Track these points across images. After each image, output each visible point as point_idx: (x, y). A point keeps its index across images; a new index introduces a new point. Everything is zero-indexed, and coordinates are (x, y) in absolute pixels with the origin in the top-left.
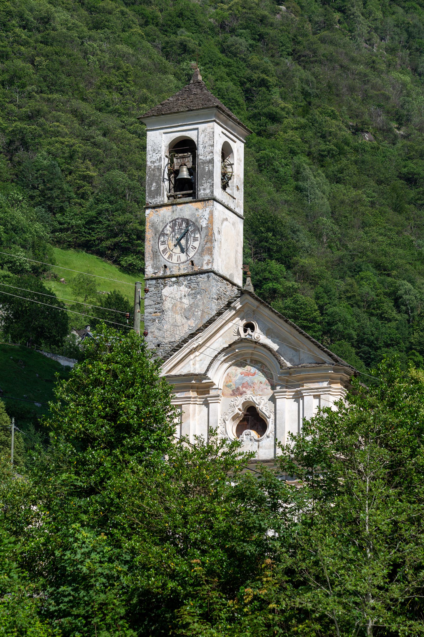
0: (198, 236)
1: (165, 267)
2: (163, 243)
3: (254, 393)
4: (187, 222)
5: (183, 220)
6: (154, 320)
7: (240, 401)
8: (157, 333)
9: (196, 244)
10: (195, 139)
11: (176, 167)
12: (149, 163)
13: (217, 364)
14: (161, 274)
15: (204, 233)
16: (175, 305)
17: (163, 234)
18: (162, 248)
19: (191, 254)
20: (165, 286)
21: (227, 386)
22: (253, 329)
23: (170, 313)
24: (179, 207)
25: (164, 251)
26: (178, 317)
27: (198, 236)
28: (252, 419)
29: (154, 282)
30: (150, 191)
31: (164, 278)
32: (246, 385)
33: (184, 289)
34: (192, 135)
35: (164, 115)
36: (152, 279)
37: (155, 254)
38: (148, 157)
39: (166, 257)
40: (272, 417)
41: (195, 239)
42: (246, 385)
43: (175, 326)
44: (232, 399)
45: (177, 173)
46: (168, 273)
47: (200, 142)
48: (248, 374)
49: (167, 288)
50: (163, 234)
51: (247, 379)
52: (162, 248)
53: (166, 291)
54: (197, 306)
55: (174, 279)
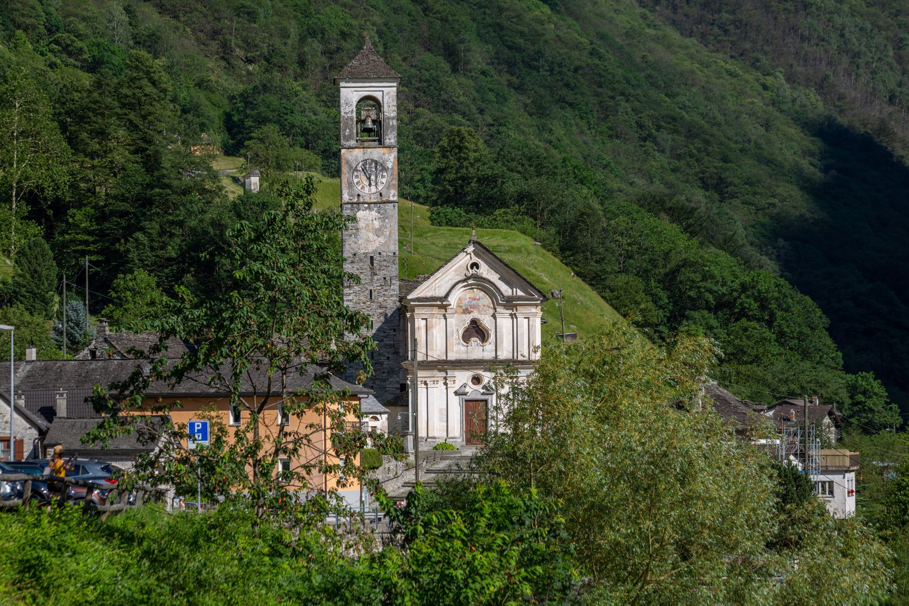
0: (385, 174)
1: (359, 195)
2: (357, 177)
3: (479, 311)
4: (376, 163)
5: (372, 160)
6: (351, 235)
7: (468, 318)
8: (353, 245)
9: (384, 180)
10: (380, 99)
11: (363, 118)
12: (342, 114)
13: (453, 292)
14: (355, 200)
15: (390, 172)
16: (367, 225)
17: (356, 170)
18: (356, 180)
19: (380, 188)
20: (359, 210)
21: (458, 306)
22: (478, 268)
23: (363, 231)
24: (369, 150)
25: (357, 183)
26: (371, 235)
27: (385, 174)
28: (476, 331)
29: (349, 206)
30: (345, 136)
31: (358, 203)
32: (473, 307)
33: (374, 214)
34: (378, 95)
35: (357, 77)
36: (348, 203)
37: (350, 185)
38: (342, 109)
39: (359, 188)
40: (493, 330)
41: (383, 177)
42: (473, 307)
43: (368, 241)
44: (463, 316)
45: (364, 122)
46: (361, 200)
47: (385, 102)
48: (474, 299)
49: (360, 212)
50: (356, 170)
51: (474, 302)
52: (356, 180)
53: (360, 214)
54: (386, 227)
55: (366, 205)
